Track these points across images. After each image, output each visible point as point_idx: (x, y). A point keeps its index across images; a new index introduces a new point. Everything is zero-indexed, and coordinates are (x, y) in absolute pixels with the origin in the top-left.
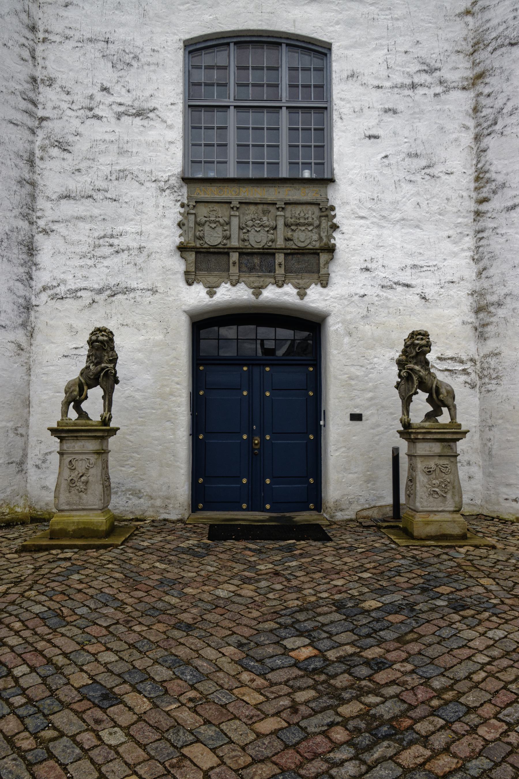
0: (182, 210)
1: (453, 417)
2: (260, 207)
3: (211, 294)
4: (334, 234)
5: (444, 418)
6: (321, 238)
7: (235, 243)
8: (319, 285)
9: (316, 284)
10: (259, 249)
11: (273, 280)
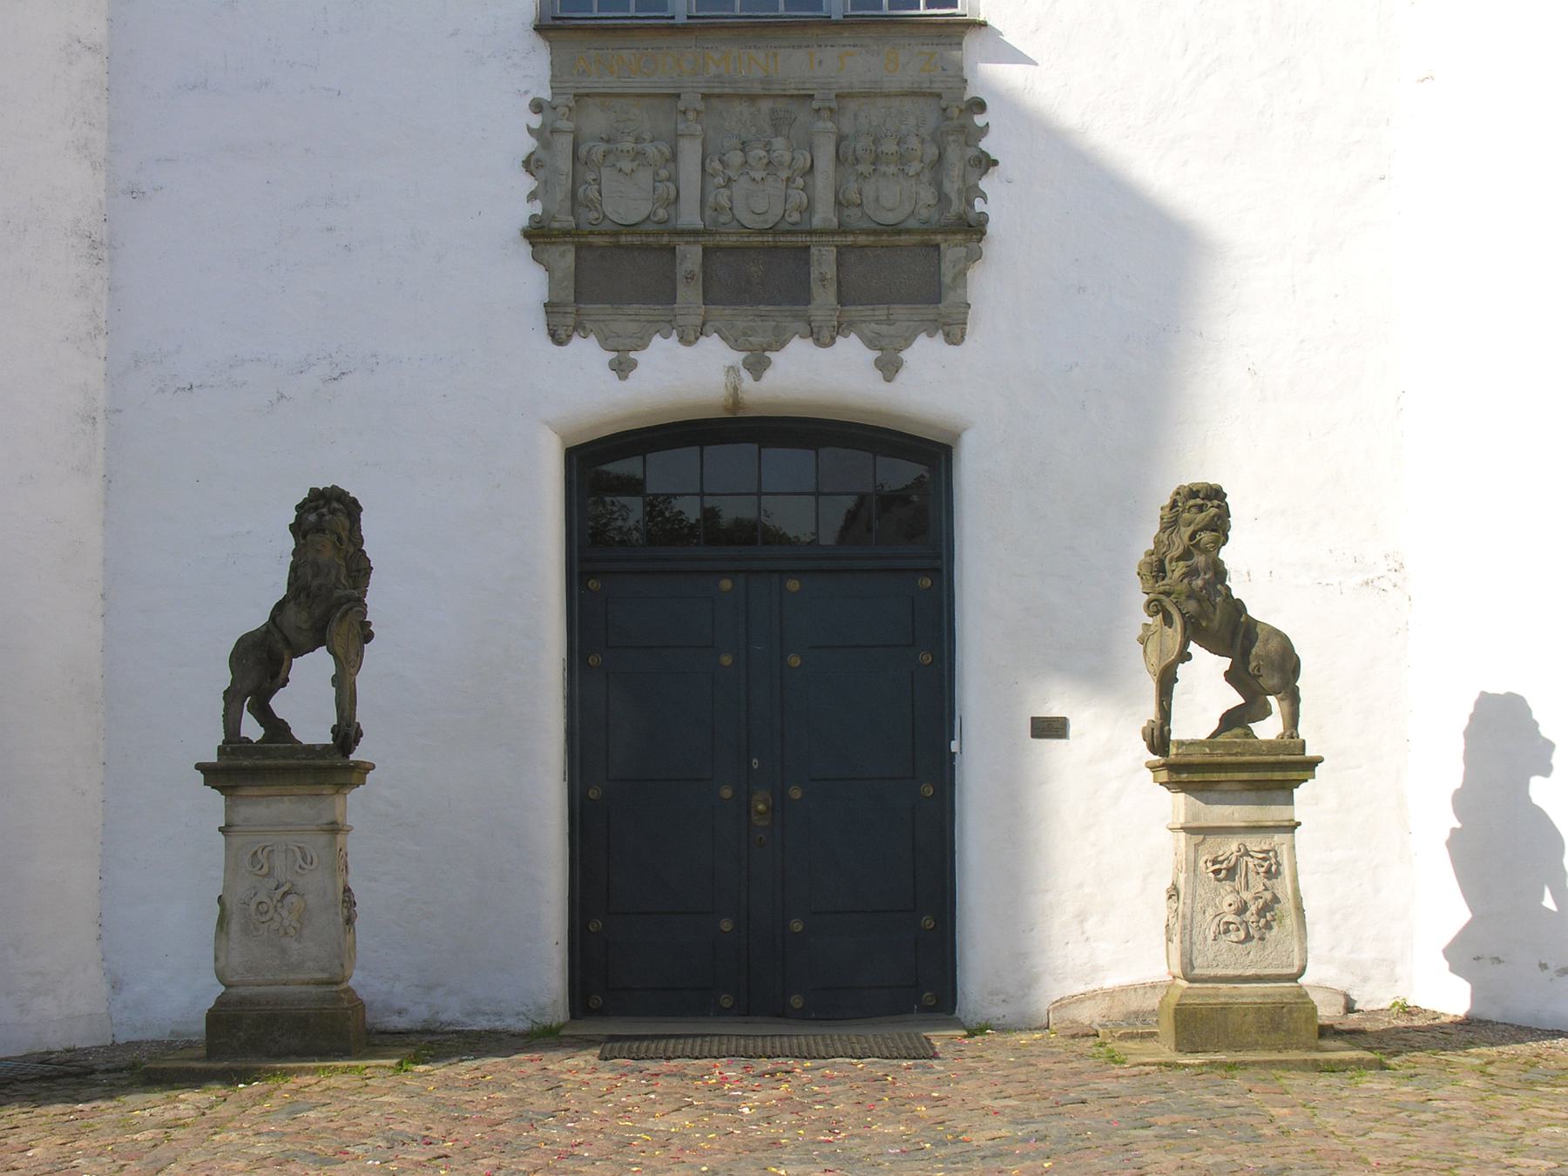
0: (536, 121)
1: (1293, 719)
2: (765, 106)
3: (623, 368)
4: (984, 184)
5: (1268, 729)
6: (942, 199)
7: (689, 216)
8: (940, 336)
9: (931, 336)
10: (761, 232)
11: (801, 326)
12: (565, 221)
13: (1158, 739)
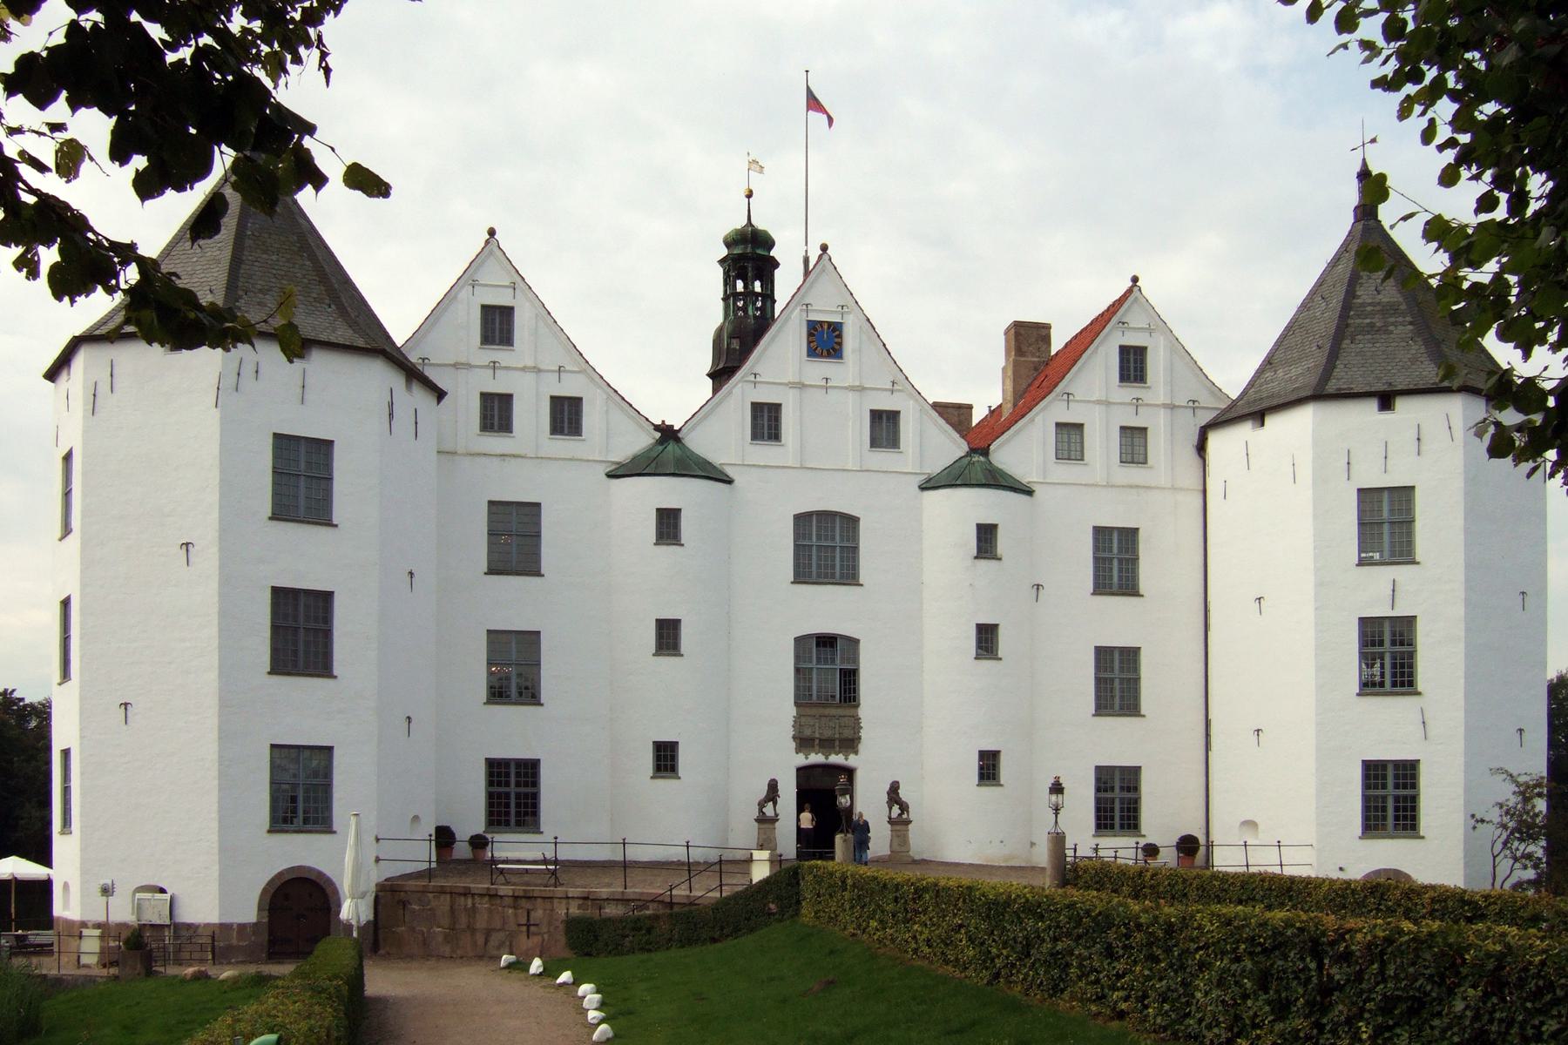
1: (908, 815)
3: (807, 758)
5: (905, 816)
7: (817, 735)
12: (797, 735)
13: (890, 818)
